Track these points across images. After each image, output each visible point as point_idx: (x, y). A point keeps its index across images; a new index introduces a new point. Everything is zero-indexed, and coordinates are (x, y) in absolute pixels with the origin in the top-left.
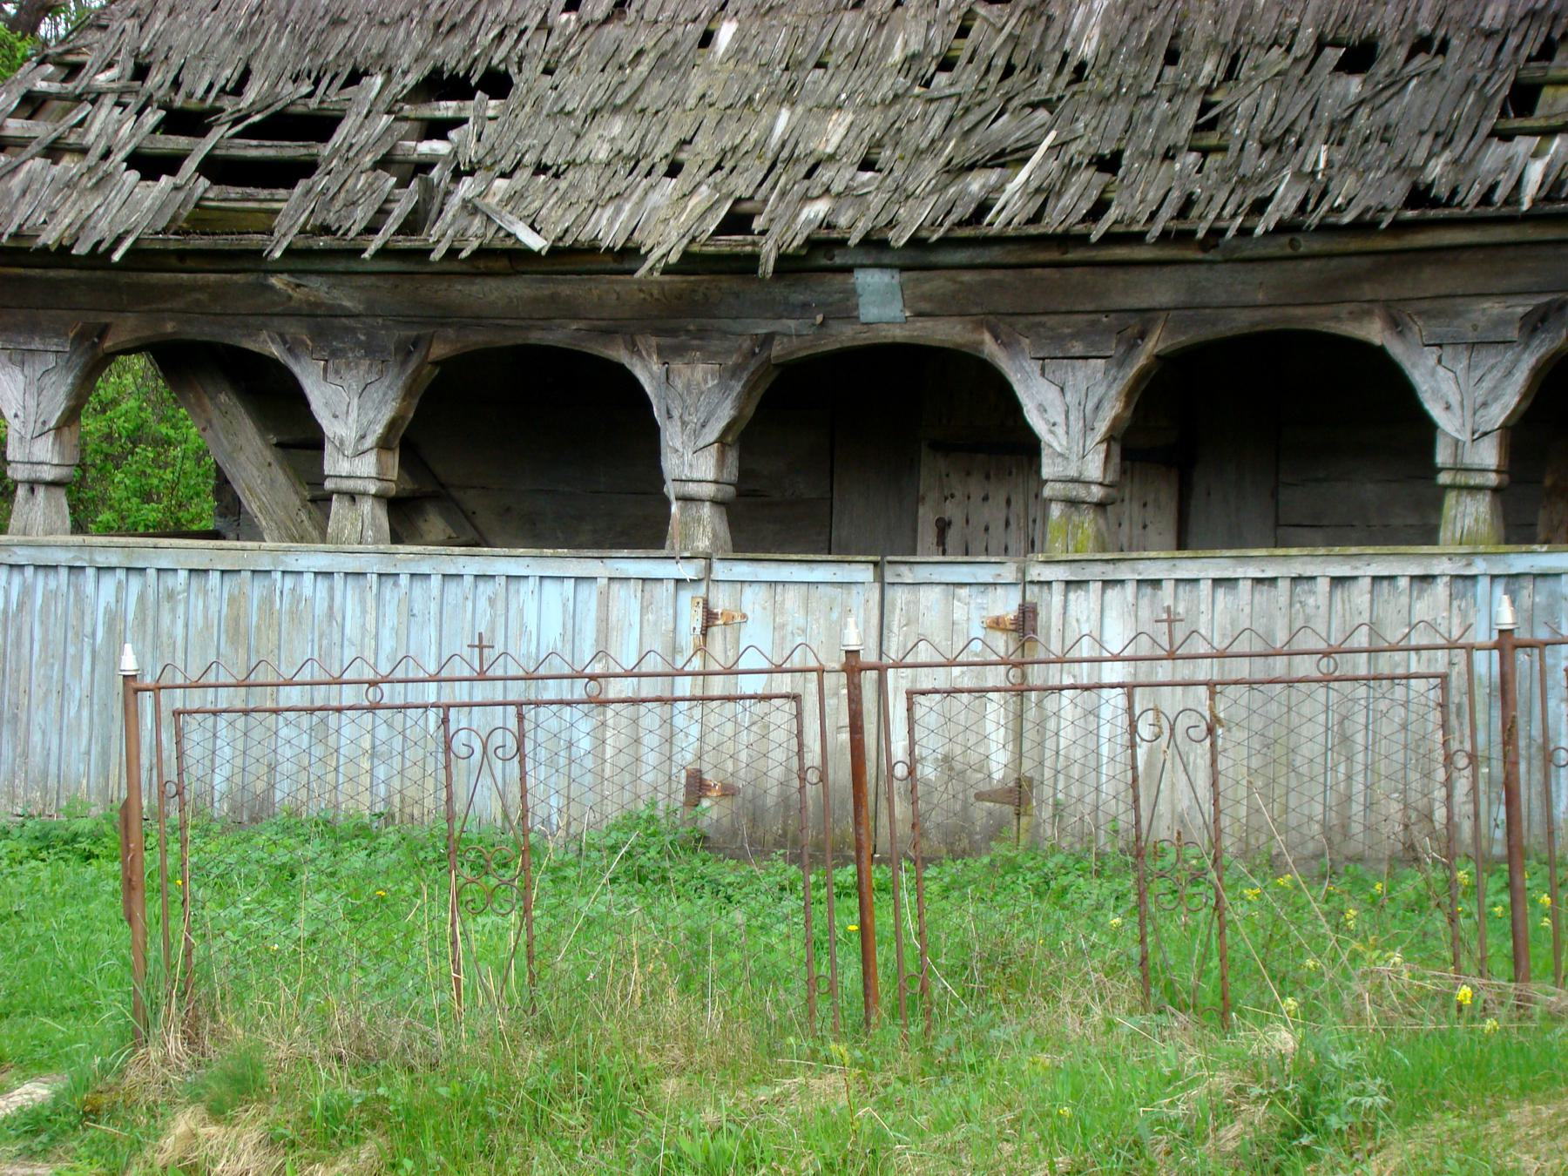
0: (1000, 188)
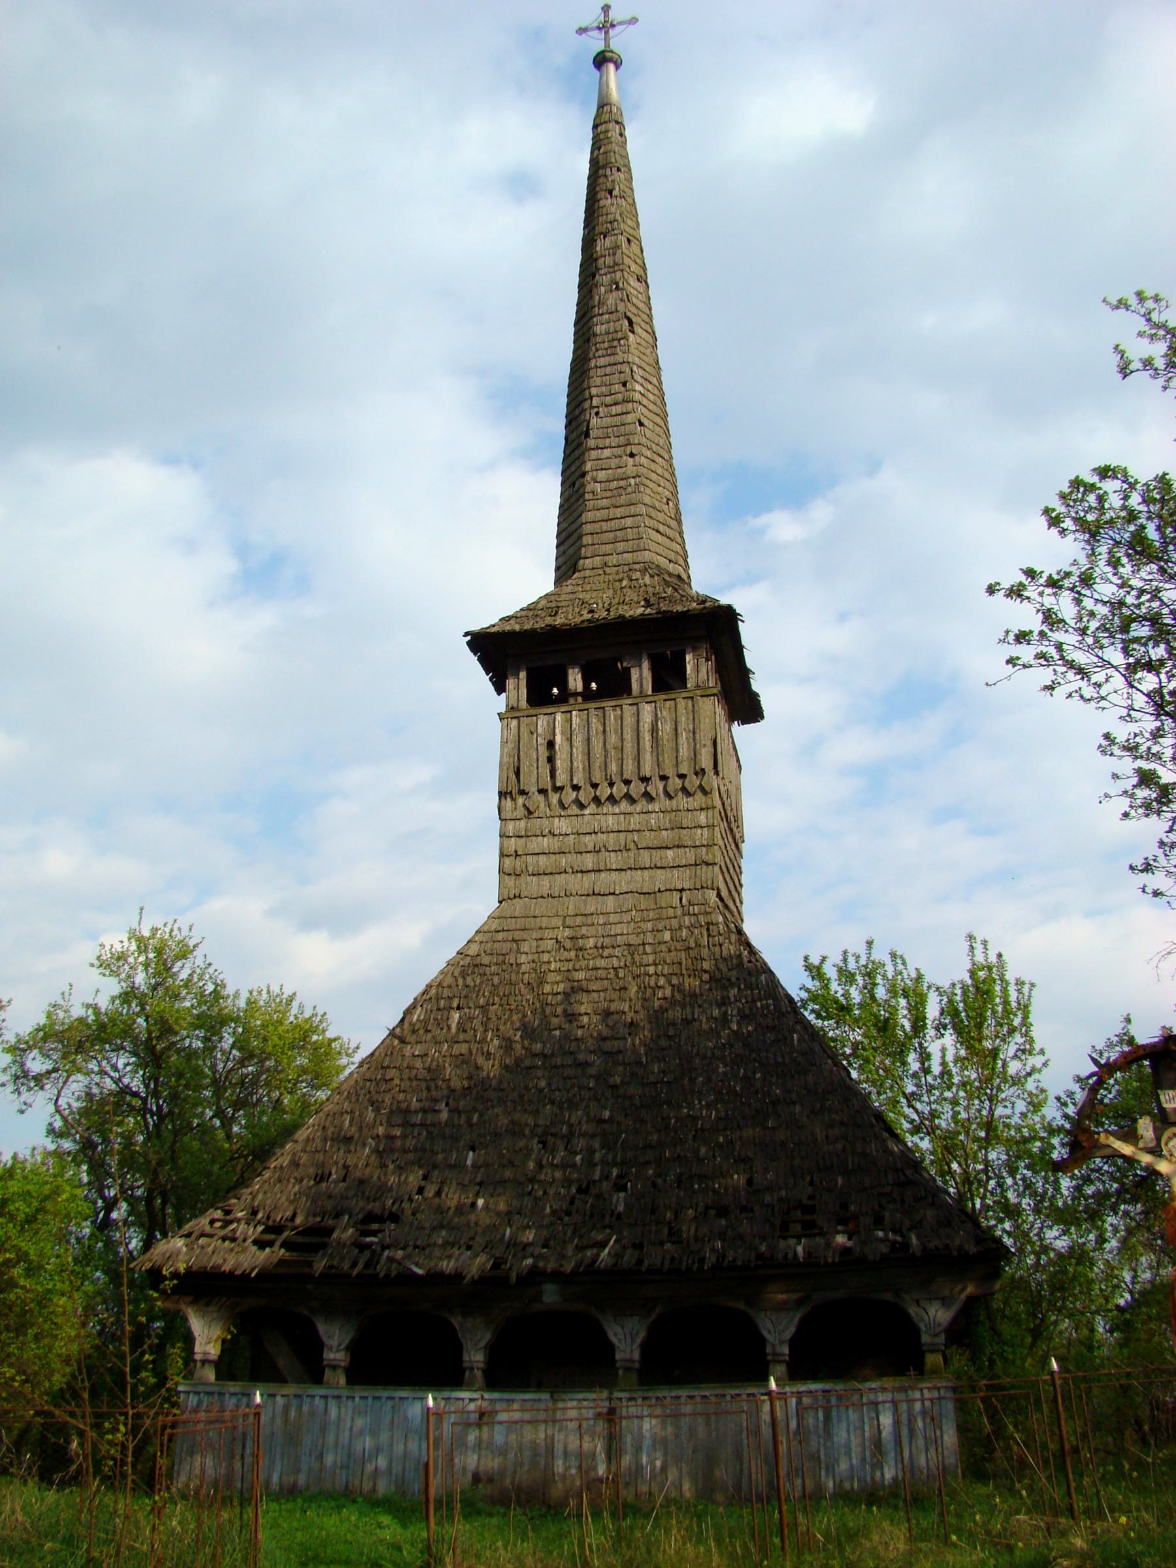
0: (598, 1255)
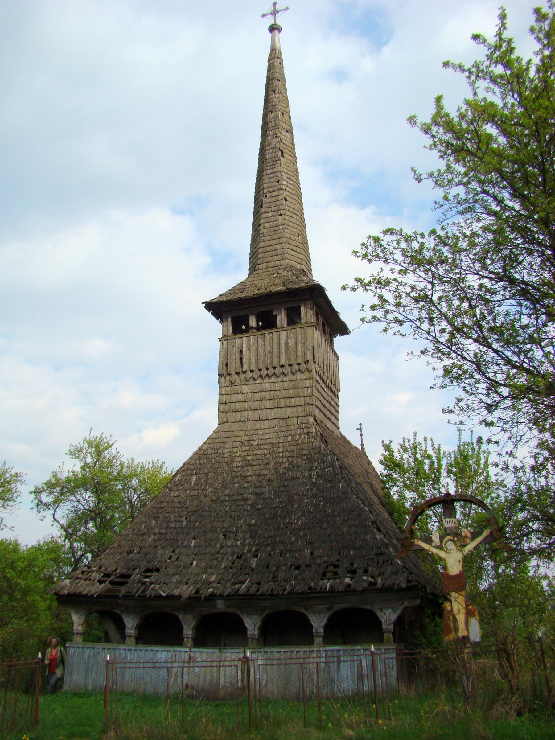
0: (241, 587)
